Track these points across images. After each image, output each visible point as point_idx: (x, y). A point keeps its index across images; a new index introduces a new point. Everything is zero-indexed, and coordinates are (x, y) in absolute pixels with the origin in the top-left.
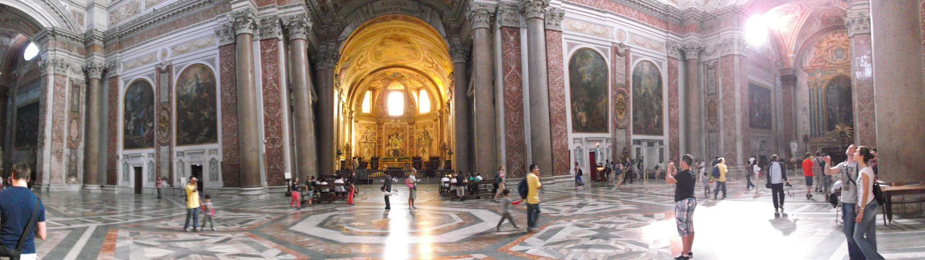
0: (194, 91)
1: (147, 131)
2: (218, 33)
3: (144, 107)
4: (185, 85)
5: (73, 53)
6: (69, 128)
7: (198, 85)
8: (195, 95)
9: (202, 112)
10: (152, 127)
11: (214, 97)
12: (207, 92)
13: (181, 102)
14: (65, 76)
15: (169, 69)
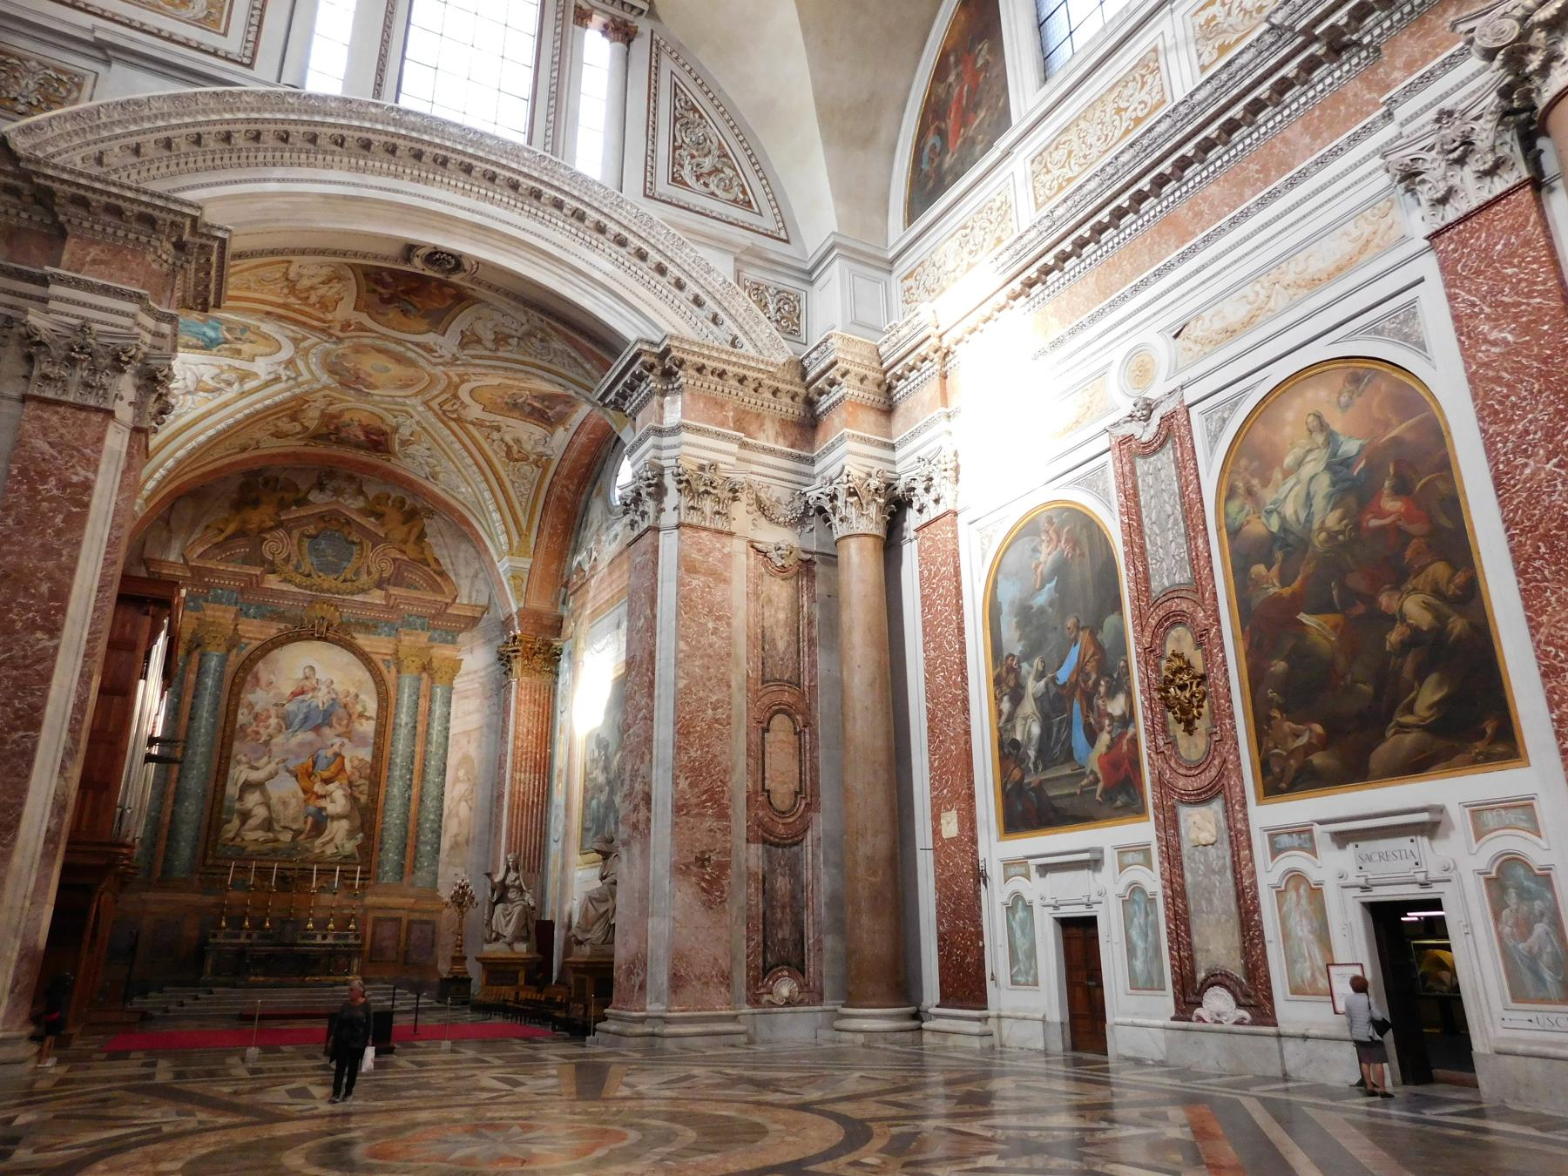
0: (1319, 503)
1: (1105, 738)
2: (1410, 176)
3: (1078, 628)
4: (1266, 482)
5: (761, 442)
6: (759, 755)
7: (1337, 466)
8: (1332, 519)
9: (1386, 601)
10: (1128, 719)
11: (1453, 504)
12: (1402, 489)
13: (1259, 569)
14: (731, 534)
15: (1173, 431)
